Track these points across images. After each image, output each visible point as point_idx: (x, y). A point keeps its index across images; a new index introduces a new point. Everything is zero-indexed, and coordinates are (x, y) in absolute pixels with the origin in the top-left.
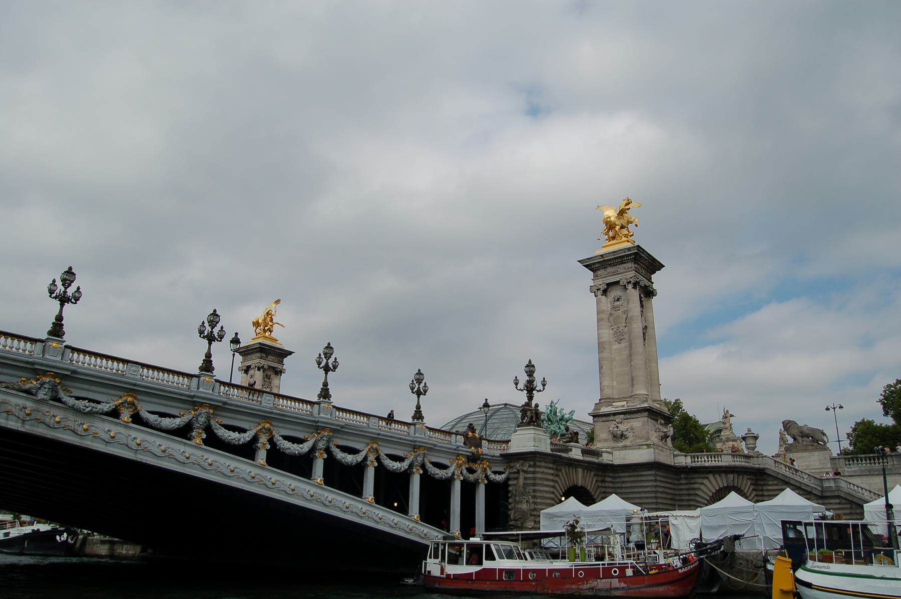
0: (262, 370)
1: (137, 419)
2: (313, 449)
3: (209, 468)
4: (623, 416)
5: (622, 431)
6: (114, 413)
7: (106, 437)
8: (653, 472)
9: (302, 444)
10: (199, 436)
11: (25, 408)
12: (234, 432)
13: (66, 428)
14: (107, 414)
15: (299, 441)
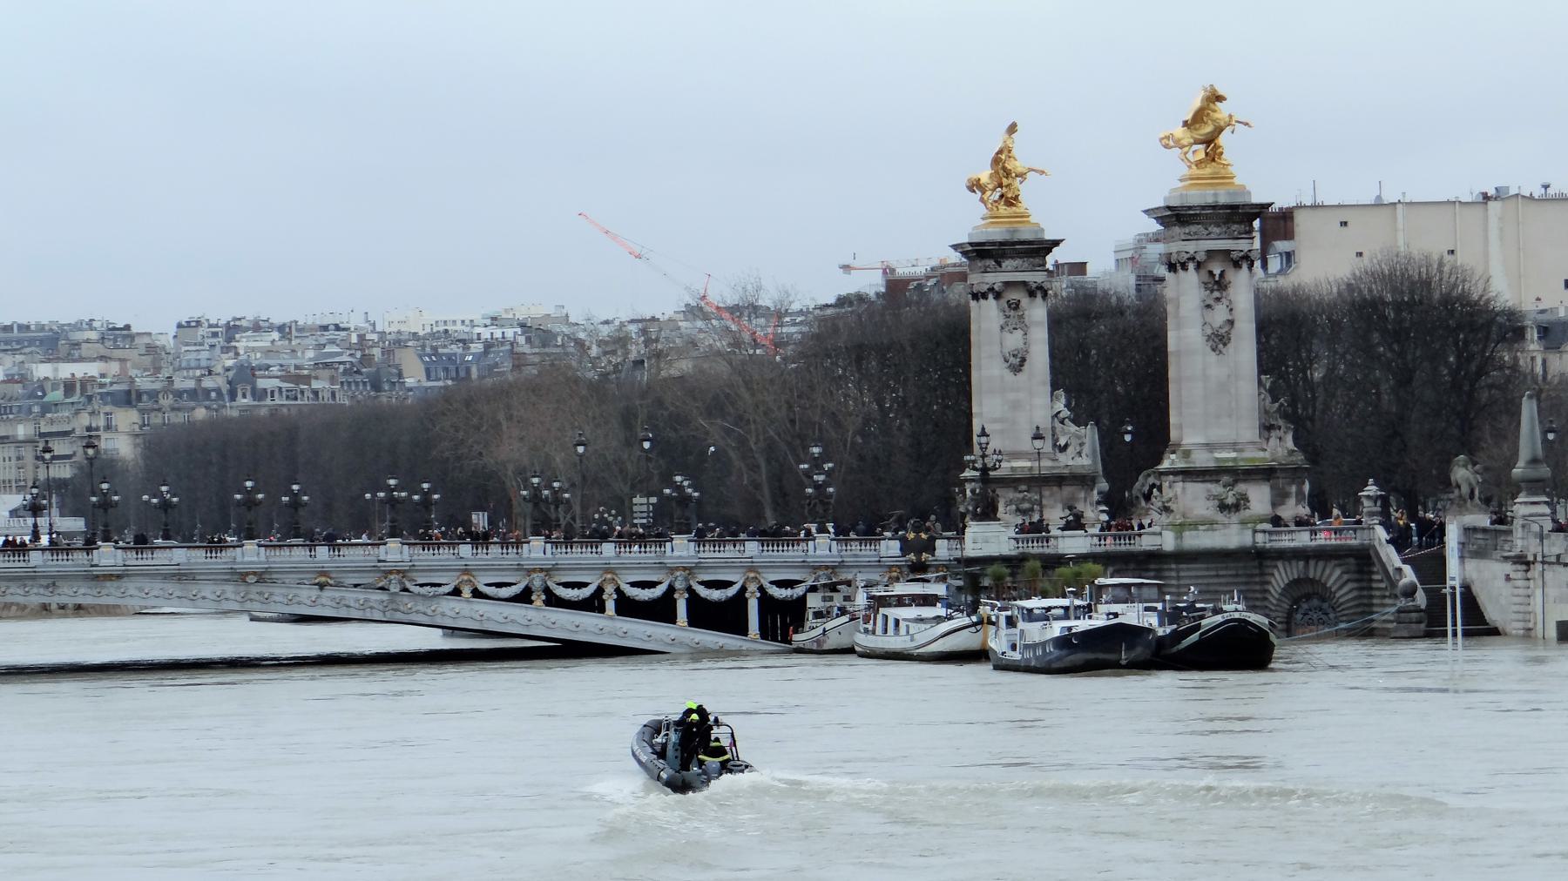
0: (991, 296)
1: (477, 594)
2: (671, 589)
3: (553, 626)
4: (1171, 476)
5: (1163, 502)
6: (456, 592)
7: (453, 614)
8: (1173, 566)
9: (655, 587)
10: (538, 598)
11: (383, 602)
12: (573, 589)
13: (417, 612)
14: (449, 594)
15: (652, 585)
